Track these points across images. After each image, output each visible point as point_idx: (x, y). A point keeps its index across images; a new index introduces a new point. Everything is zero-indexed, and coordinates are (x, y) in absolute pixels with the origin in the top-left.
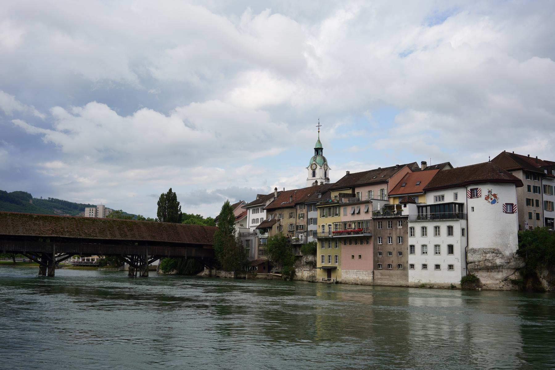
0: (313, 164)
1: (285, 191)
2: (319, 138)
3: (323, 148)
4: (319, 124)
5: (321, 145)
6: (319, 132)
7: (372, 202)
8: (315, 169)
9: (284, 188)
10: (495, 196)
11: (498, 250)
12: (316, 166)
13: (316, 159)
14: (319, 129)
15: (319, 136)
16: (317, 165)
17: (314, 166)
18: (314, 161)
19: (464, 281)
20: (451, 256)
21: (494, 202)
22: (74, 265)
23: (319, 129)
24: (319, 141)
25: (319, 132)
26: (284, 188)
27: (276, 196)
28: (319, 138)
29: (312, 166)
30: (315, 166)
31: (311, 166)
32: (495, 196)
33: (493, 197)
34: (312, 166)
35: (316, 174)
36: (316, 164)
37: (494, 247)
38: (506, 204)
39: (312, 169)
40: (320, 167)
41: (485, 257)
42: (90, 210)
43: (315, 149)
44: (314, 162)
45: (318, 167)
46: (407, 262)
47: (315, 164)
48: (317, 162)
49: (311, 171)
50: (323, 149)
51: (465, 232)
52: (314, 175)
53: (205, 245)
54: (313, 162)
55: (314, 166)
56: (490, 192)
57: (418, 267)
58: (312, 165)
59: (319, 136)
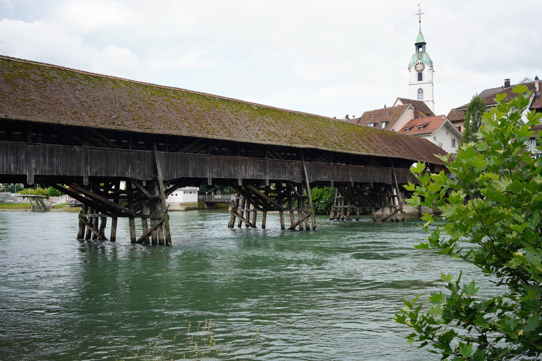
0: (418, 63)
2: (420, 29)
3: (425, 42)
4: (420, 10)
5: (424, 39)
6: (420, 22)
8: (423, 70)
12: (424, 65)
13: (421, 57)
14: (420, 18)
15: (420, 27)
16: (425, 65)
17: (420, 67)
18: (419, 59)
22: (71, 205)
23: (420, 18)
24: (420, 33)
25: (420, 22)
27: (537, 90)
28: (420, 29)
29: (417, 66)
30: (422, 67)
31: (416, 66)
34: (417, 66)
35: (423, 76)
36: (423, 64)
40: (429, 68)
43: (416, 44)
44: (420, 61)
45: (425, 68)
47: (421, 63)
48: (424, 60)
49: (416, 74)
50: (425, 44)
52: (420, 77)
53: (436, 165)
58: (417, 64)
59: (420, 27)
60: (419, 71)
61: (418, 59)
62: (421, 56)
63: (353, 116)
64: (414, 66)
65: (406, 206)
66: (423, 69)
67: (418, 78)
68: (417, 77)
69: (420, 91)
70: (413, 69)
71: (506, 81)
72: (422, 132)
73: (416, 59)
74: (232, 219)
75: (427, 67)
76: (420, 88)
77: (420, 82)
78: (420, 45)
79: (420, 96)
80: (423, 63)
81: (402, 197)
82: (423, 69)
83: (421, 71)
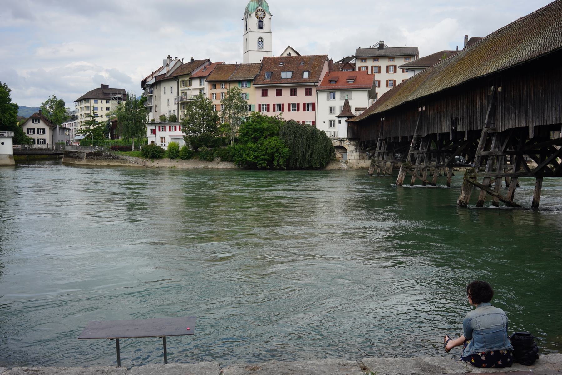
0: (259, 10)
1: (458, 50)
9: (457, 47)
12: (265, 13)
16: (266, 13)
18: (260, 5)
26: (457, 47)
29: (258, 13)
30: (263, 15)
31: (256, 13)
34: (258, 13)
35: (263, 24)
36: (263, 11)
39: (257, 18)
40: (269, 17)
44: (260, 8)
45: (266, 15)
47: (262, 10)
48: (264, 8)
54: (257, 7)
55: (260, 14)
58: (257, 11)
60: (259, 18)
61: (258, 5)
62: (261, 2)
63: (176, 58)
64: (255, 12)
65: (363, 161)
66: (264, 17)
67: (258, 26)
68: (258, 24)
69: (260, 40)
70: (253, 15)
71: (381, 43)
72: (358, 86)
73: (256, 5)
74: (402, 177)
75: (267, 16)
76: (260, 37)
77: (261, 30)
79: (260, 45)
80: (264, 10)
81: (359, 151)
82: (264, 17)
83: (261, 18)
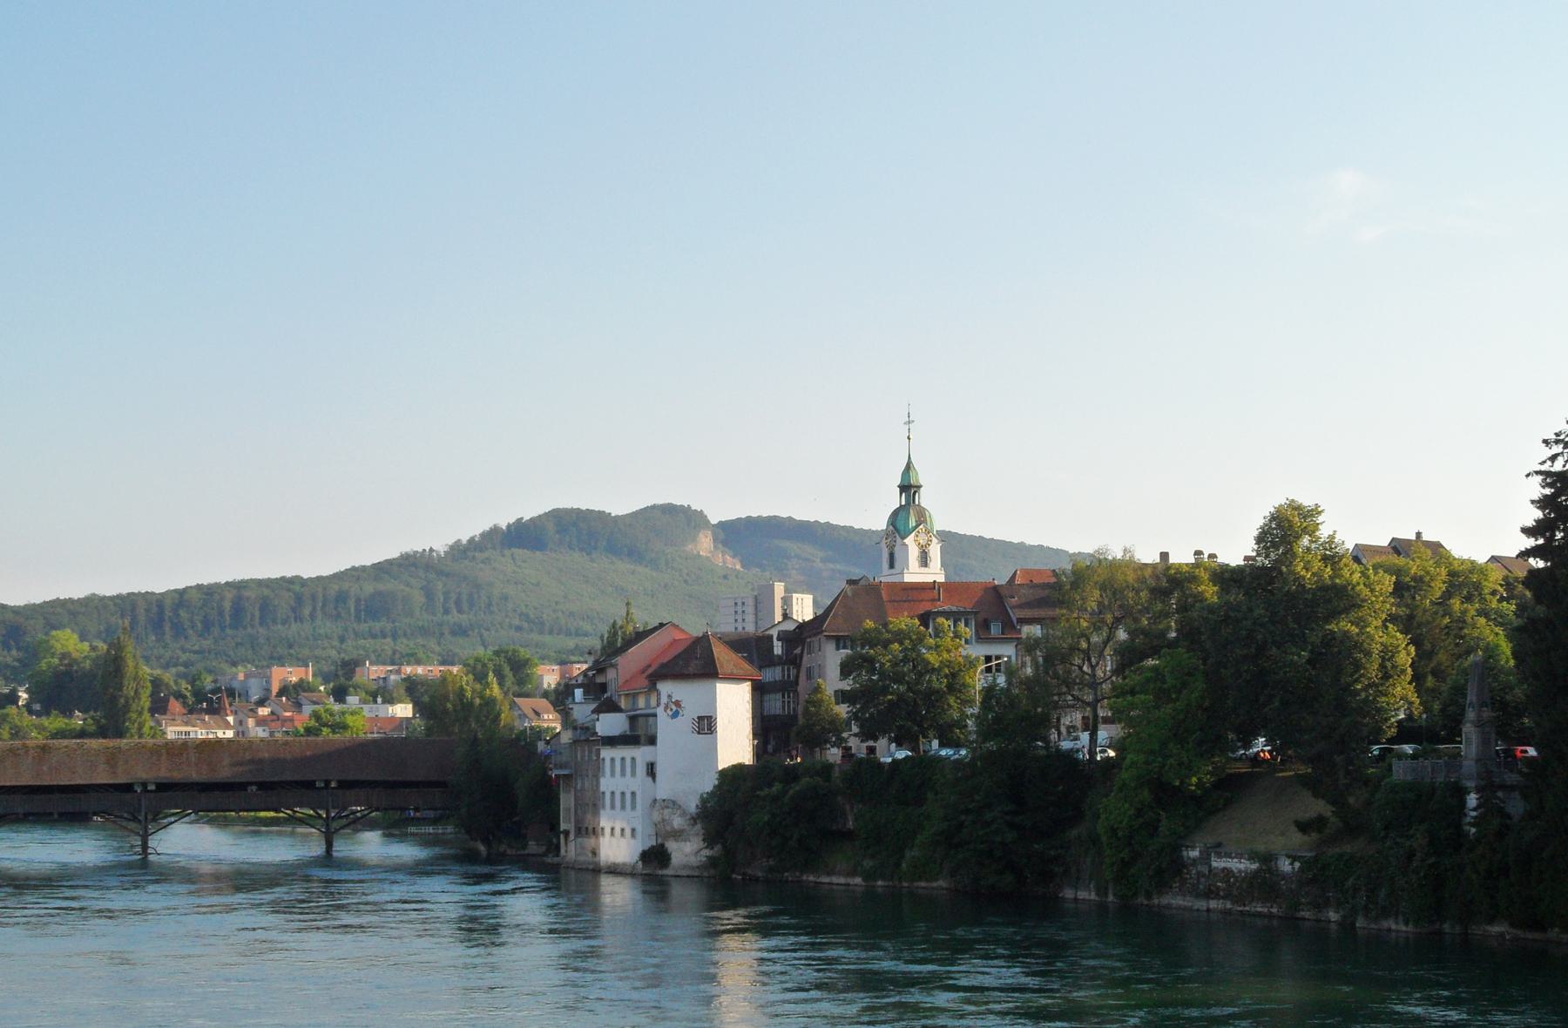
6: (909, 438)
7: (572, 709)
10: (677, 704)
11: (674, 803)
19: (646, 856)
20: (633, 814)
21: (675, 715)
32: (677, 704)
33: (674, 708)
37: (673, 798)
38: (699, 718)
41: (662, 814)
42: (736, 604)
43: (899, 486)
46: (599, 824)
51: (651, 770)
56: (670, 696)
57: (608, 831)
77: (893, 571)
78: (908, 488)
